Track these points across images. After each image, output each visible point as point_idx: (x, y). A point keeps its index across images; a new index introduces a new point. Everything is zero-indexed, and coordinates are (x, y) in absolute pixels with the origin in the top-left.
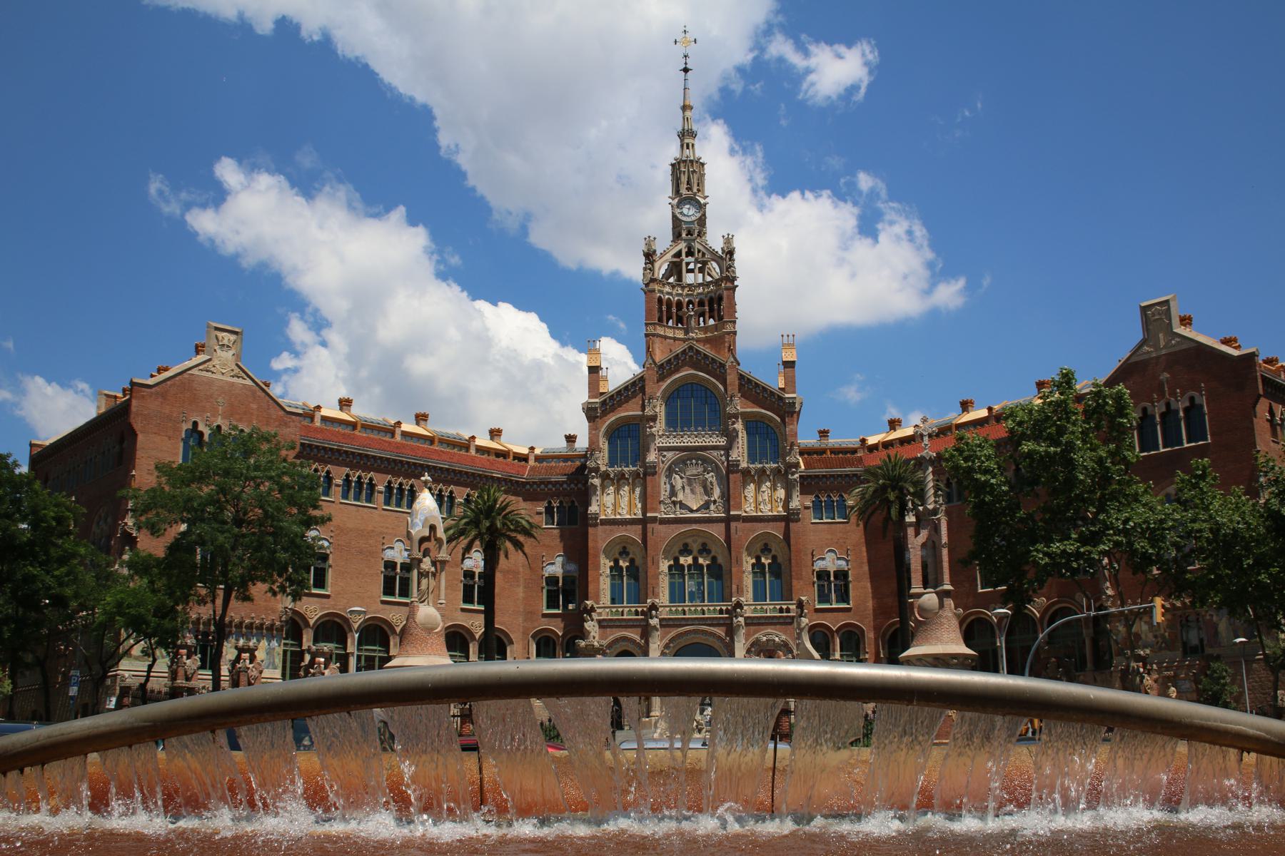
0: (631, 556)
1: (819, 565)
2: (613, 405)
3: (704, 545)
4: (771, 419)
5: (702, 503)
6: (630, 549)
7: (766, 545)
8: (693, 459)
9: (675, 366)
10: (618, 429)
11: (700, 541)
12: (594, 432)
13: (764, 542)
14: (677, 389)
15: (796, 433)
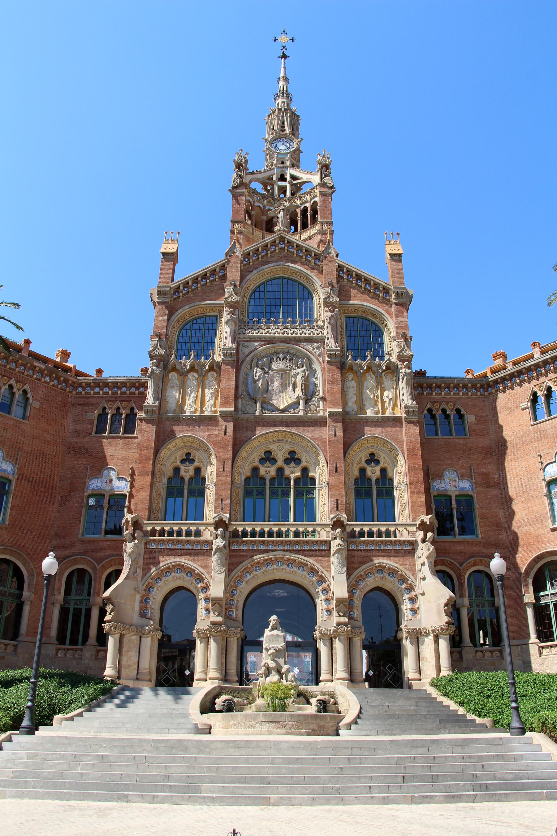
0: (196, 464)
1: (439, 486)
2: (188, 292)
3: (292, 453)
4: (375, 314)
5: (290, 402)
6: (196, 455)
7: (372, 455)
8: (280, 353)
9: (262, 257)
10: (190, 322)
11: (288, 447)
12: (161, 318)
13: (370, 451)
14: (264, 283)
15: (407, 326)
